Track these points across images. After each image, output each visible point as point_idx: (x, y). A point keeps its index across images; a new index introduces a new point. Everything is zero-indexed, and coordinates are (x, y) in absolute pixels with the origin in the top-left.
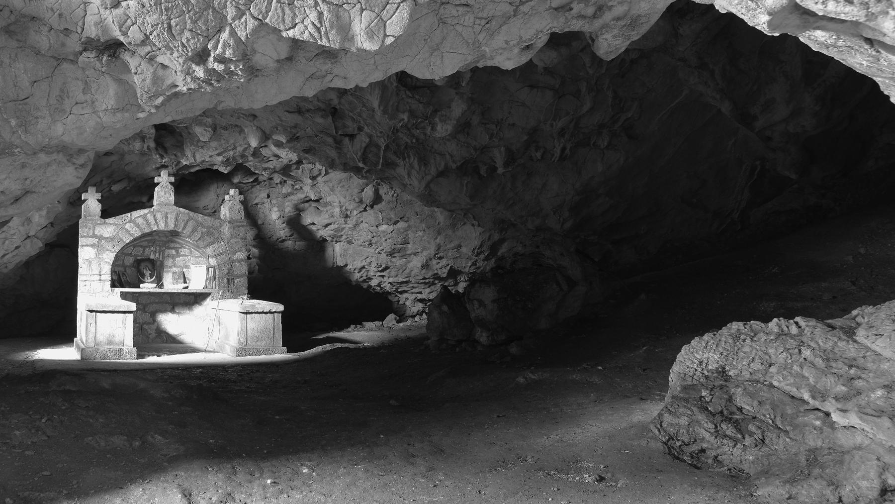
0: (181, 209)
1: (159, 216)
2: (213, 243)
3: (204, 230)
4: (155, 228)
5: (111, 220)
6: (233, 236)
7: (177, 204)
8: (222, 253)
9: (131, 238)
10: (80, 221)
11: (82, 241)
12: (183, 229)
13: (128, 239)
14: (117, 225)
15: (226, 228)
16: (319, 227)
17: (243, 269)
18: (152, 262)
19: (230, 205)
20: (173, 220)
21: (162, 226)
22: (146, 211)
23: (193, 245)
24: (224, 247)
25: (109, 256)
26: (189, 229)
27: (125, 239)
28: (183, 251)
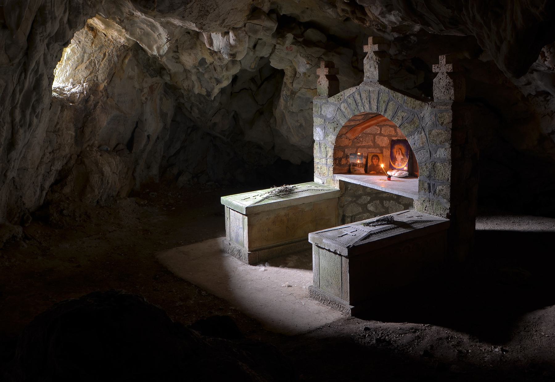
0: (382, 87)
1: (364, 95)
3: (404, 114)
4: (362, 111)
5: (332, 99)
6: (434, 125)
7: (382, 81)
8: (423, 148)
9: (346, 120)
13: (343, 122)
14: (336, 105)
17: (445, 172)
20: (376, 101)
21: (367, 110)
22: (353, 89)
24: (425, 140)
27: (341, 122)
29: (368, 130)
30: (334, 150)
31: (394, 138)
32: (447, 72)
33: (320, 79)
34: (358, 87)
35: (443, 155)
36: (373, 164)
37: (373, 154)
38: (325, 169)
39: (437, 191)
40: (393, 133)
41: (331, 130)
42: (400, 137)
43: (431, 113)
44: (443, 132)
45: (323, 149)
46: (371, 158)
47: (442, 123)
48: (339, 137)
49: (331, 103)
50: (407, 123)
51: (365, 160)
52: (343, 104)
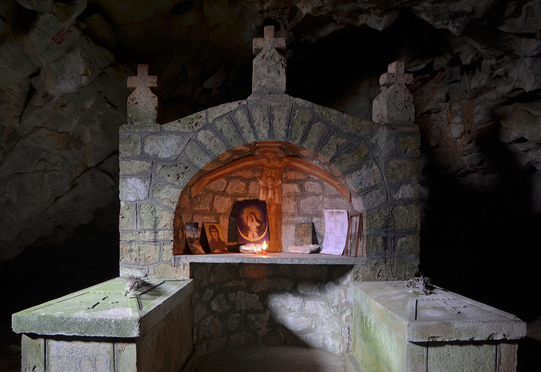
2: (358, 168)
3: (342, 141)
4: (251, 140)
6: (394, 154)
9: (208, 159)
10: (124, 131)
11: (124, 166)
12: (303, 139)
15: (382, 139)
16: (531, 145)
18: (262, 206)
19: (388, 97)
23: (324, 172)
25: (170, 194)
26: (313, 139)
27: (196, 162)
28: (312, 186)
29: (212, 186)
30: (175, 213)
31: (240, 199)
32: (406, 84)
33: (136, 94)
34: (244, 102)
35: (408, 193)
36: (213, 239)
37: (209, 224)
38: (151, 251)
39: (399, 245)
40: (242, 191)
41: (169, 179)
42: (251, 197)
43: (388, 139)
44: (407, 162)
45: (145, 214)
46: (208, 230)
47: (406, 150)
48: (186, 191)
49: (172, 133)
50: (346, 152)
51: (199, 233)
52: (202, 132)
